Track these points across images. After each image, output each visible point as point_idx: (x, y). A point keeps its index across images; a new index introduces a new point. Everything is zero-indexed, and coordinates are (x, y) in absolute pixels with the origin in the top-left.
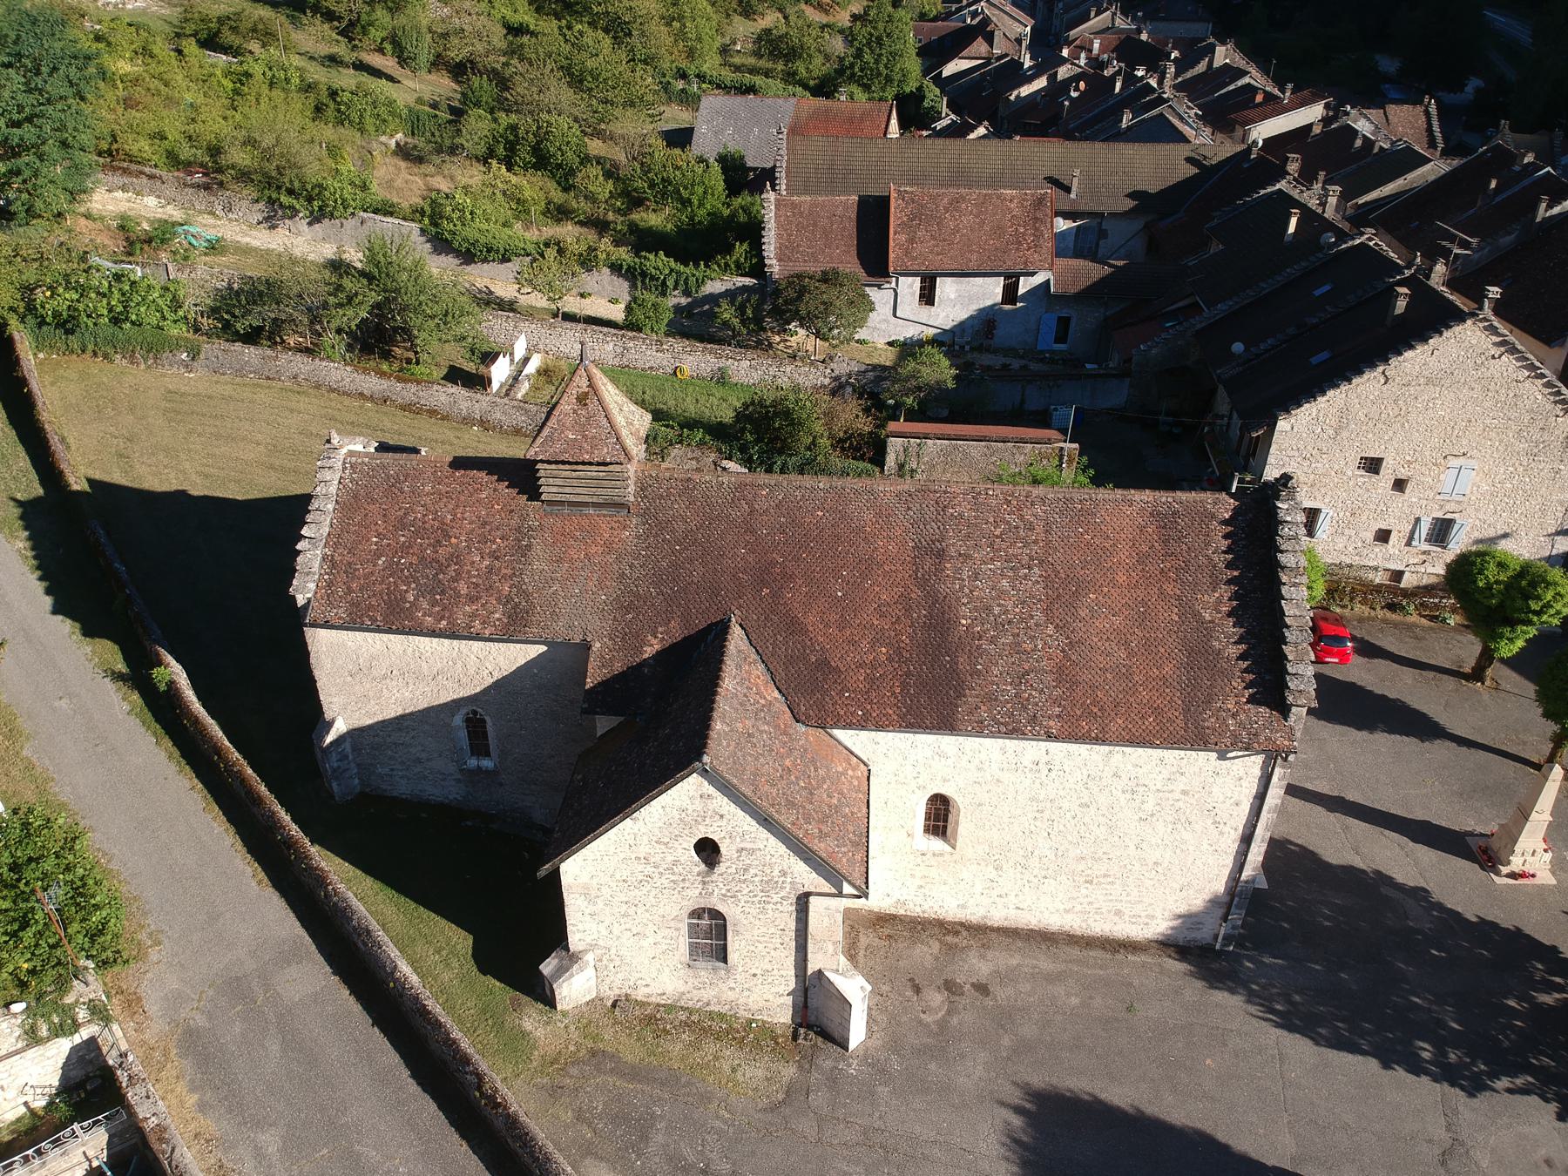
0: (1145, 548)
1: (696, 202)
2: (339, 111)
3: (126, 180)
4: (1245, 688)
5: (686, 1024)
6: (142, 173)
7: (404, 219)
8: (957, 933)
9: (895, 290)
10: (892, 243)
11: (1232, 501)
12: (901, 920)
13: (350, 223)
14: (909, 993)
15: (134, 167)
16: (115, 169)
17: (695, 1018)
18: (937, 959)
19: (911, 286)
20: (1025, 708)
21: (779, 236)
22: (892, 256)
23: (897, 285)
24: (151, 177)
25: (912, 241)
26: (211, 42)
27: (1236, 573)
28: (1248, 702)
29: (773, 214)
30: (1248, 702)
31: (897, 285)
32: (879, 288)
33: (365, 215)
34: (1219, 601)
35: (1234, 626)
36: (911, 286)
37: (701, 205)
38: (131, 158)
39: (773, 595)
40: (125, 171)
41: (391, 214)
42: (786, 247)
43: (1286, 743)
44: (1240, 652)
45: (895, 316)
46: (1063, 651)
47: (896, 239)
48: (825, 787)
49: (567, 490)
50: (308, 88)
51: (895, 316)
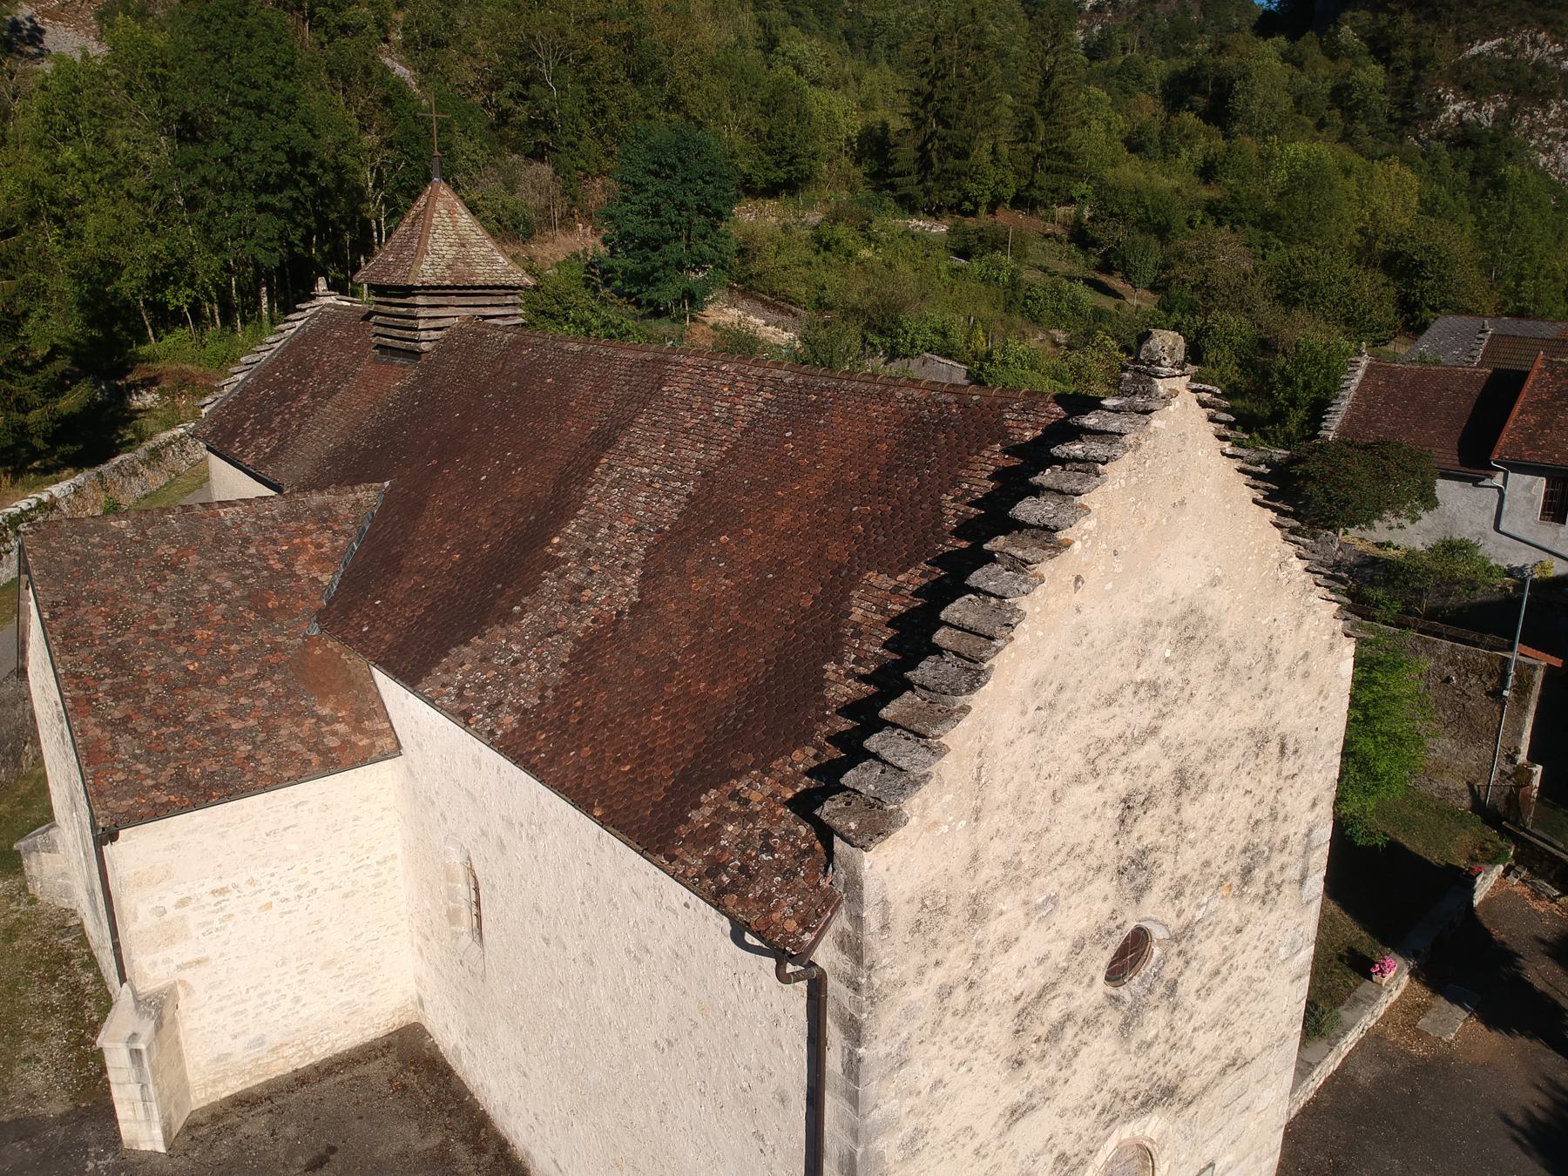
0: (853, 476)
1: (1300, 381)
2: (1025, 304)
3: (780, 318)
4: (810, 773)
5: (76, 988)
6: (790, 311)
7: (959, 362)
8: (479, 1150)
9: (1500, 490)
10: (1510, 425)
11: (1059, 409)
12: (447, 1082)
13: (916, 362)
14: (302, 1160)
15: (788, 306)
16: (775, 307)
17: (89, 989)
18: (404, 1154)
19: (1528, 487)
20: (503, 685)
21: (1355, 406)
22: (1504, 439)
23: (1505, 483)
24: (795, 315)
25: (1542, 425)
26: (965, 254)
27: (964, 544)
28: (789, 804)
29: (1357, 381)
30: (789, 804)
31: (1505, 483)
32: (1476, 485)
33: (927, 355)
34: (896, 590)
35: (885, 645)
36: (1528, 487)
37: (1307, 386)
38: (787, 299)
39: (436, 469)
40: (782, 311)
41: (949, 356)
42: (1360, 420)
43: (791, 925)
44: (857, 696)
45: (1497, 528)
46: (619, 614)
47: (1520, 418)
48: (242, 700)
49: (395, 332)
50: (1014, 284)
51: (1497, 528)
